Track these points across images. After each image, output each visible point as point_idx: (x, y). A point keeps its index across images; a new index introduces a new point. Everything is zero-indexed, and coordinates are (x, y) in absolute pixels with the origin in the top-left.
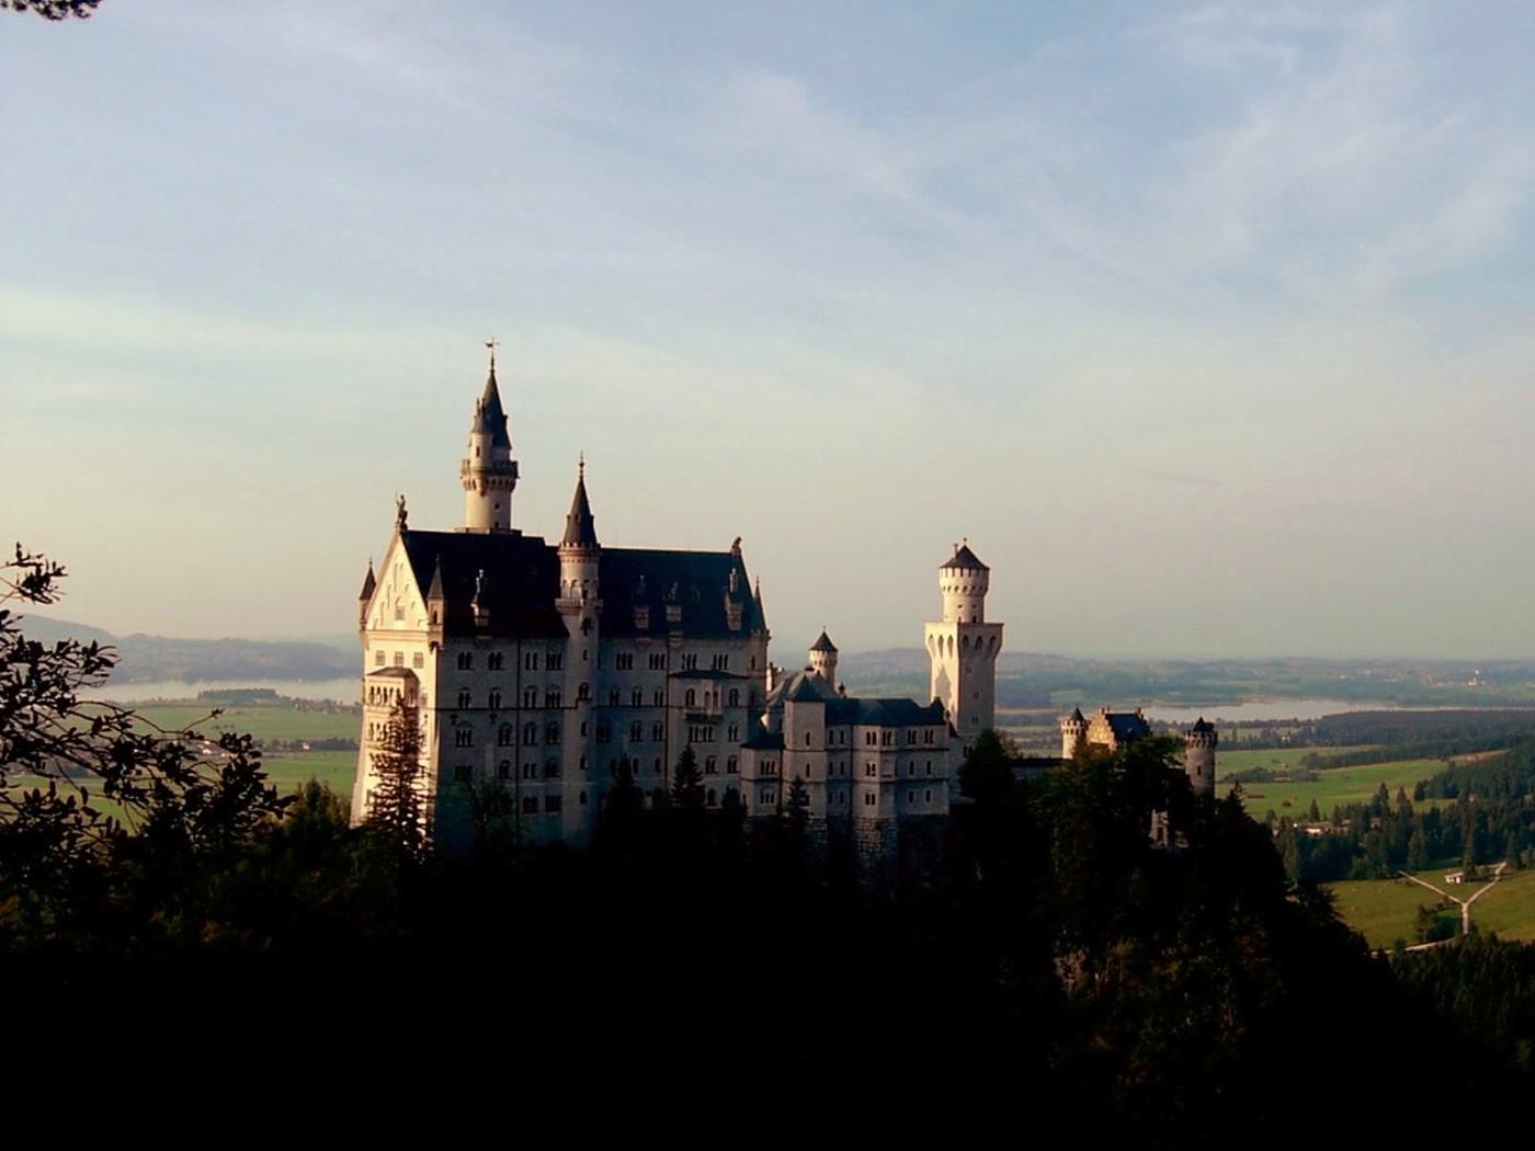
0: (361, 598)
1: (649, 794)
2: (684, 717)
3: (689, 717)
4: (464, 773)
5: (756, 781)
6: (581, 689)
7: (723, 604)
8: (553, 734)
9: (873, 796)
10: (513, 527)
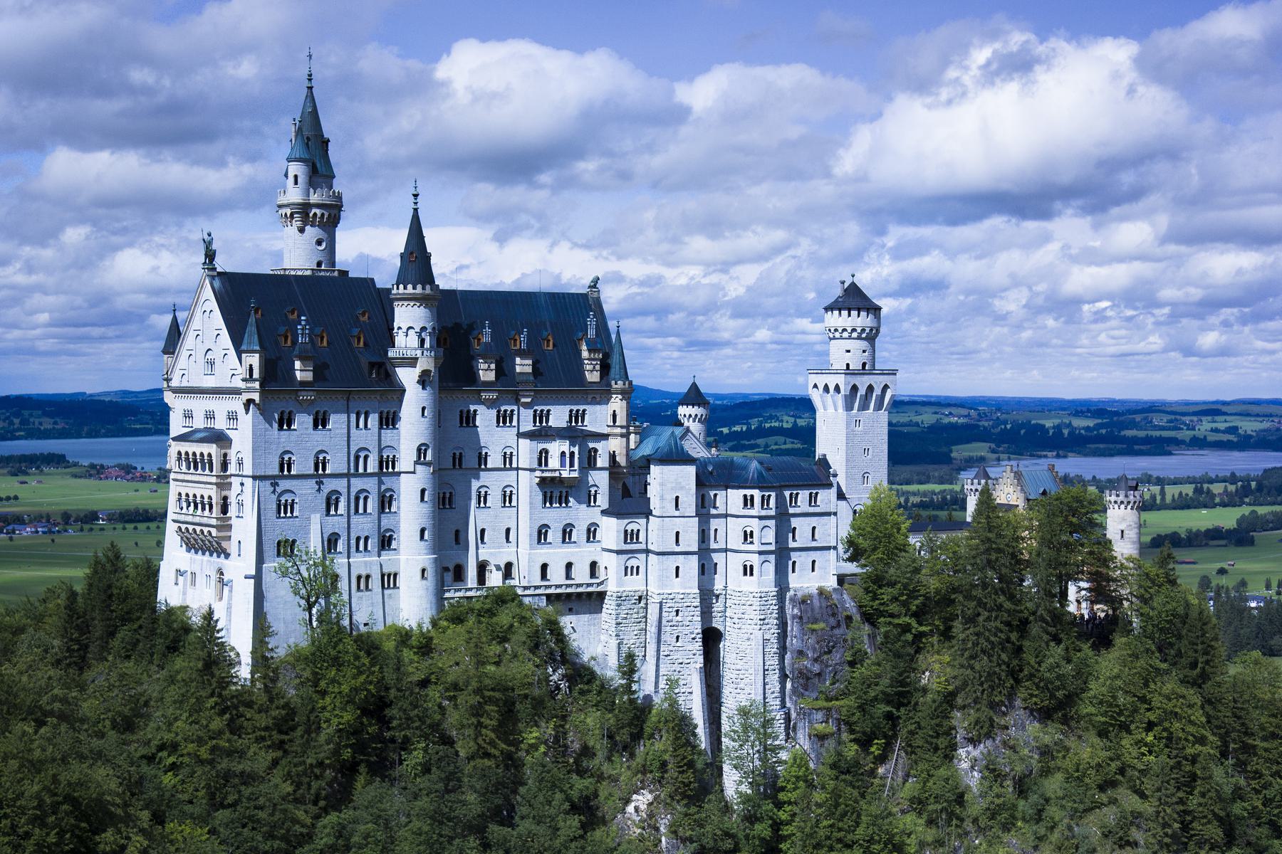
0: (165, 351)
1: (498, 568)
2: (537, 480)
3: (543, 480)
4: (286, 548)
5: (619, 552)
6: (419, 450)
7: (579, 352)
8: (386, 501)
9: (751, 567)
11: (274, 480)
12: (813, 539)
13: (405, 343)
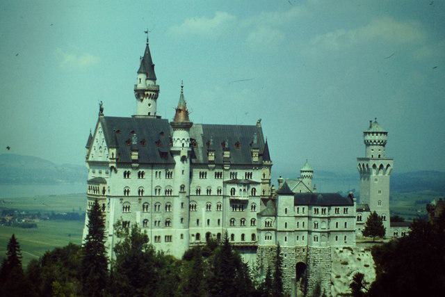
8: (168, 207)
10: (158, 114)
11: (121, 198)
12: (346, 227)
13: (177, 145)
